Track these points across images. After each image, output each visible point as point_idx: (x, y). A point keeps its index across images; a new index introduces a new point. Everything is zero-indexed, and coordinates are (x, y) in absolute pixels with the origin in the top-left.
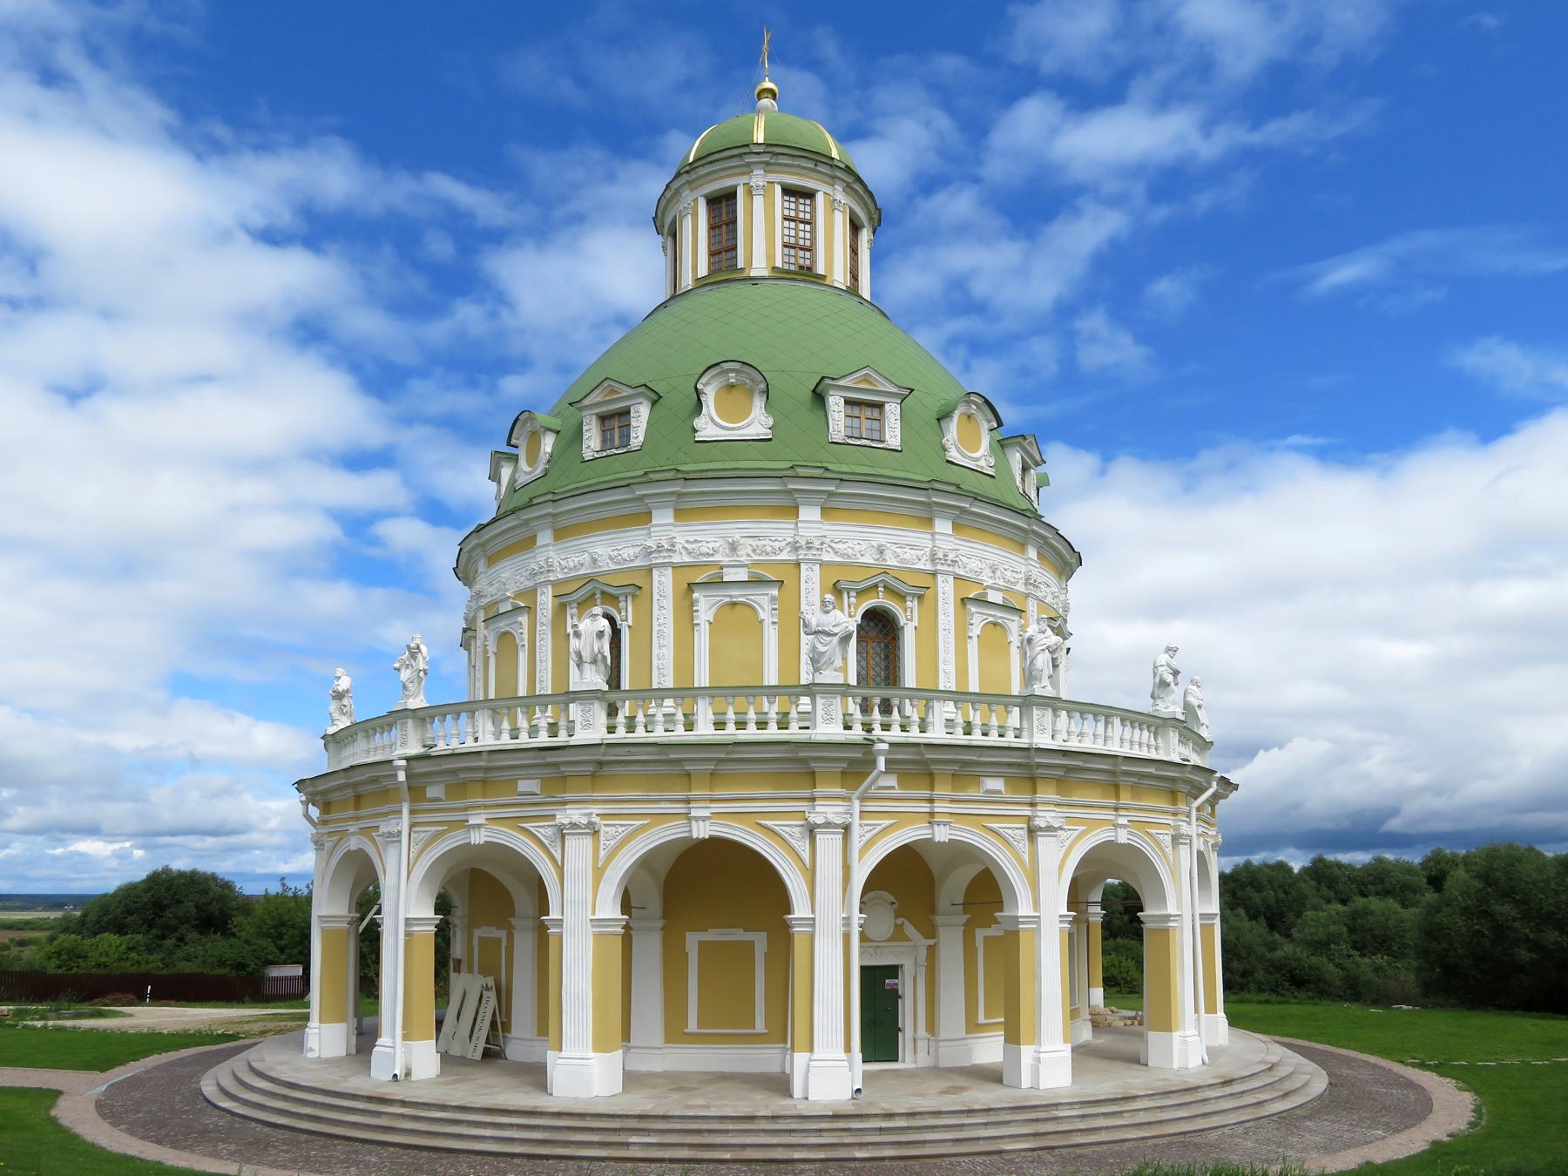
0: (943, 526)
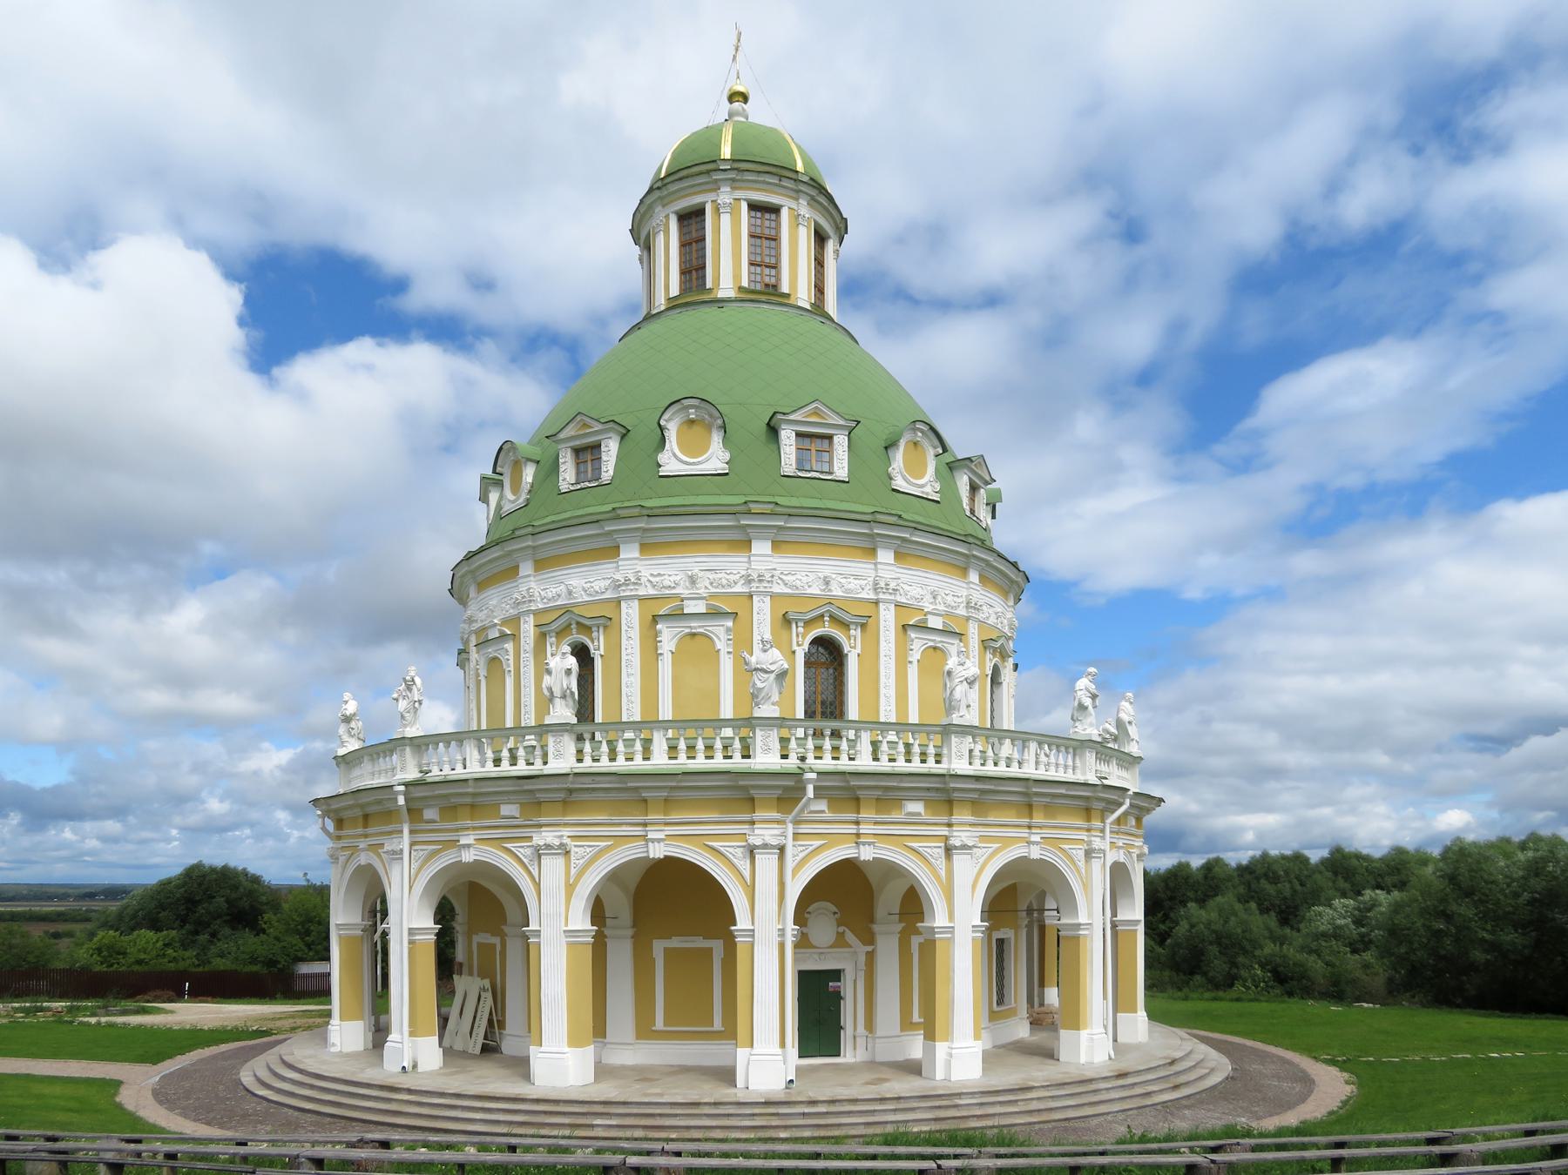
0: (885, 556)
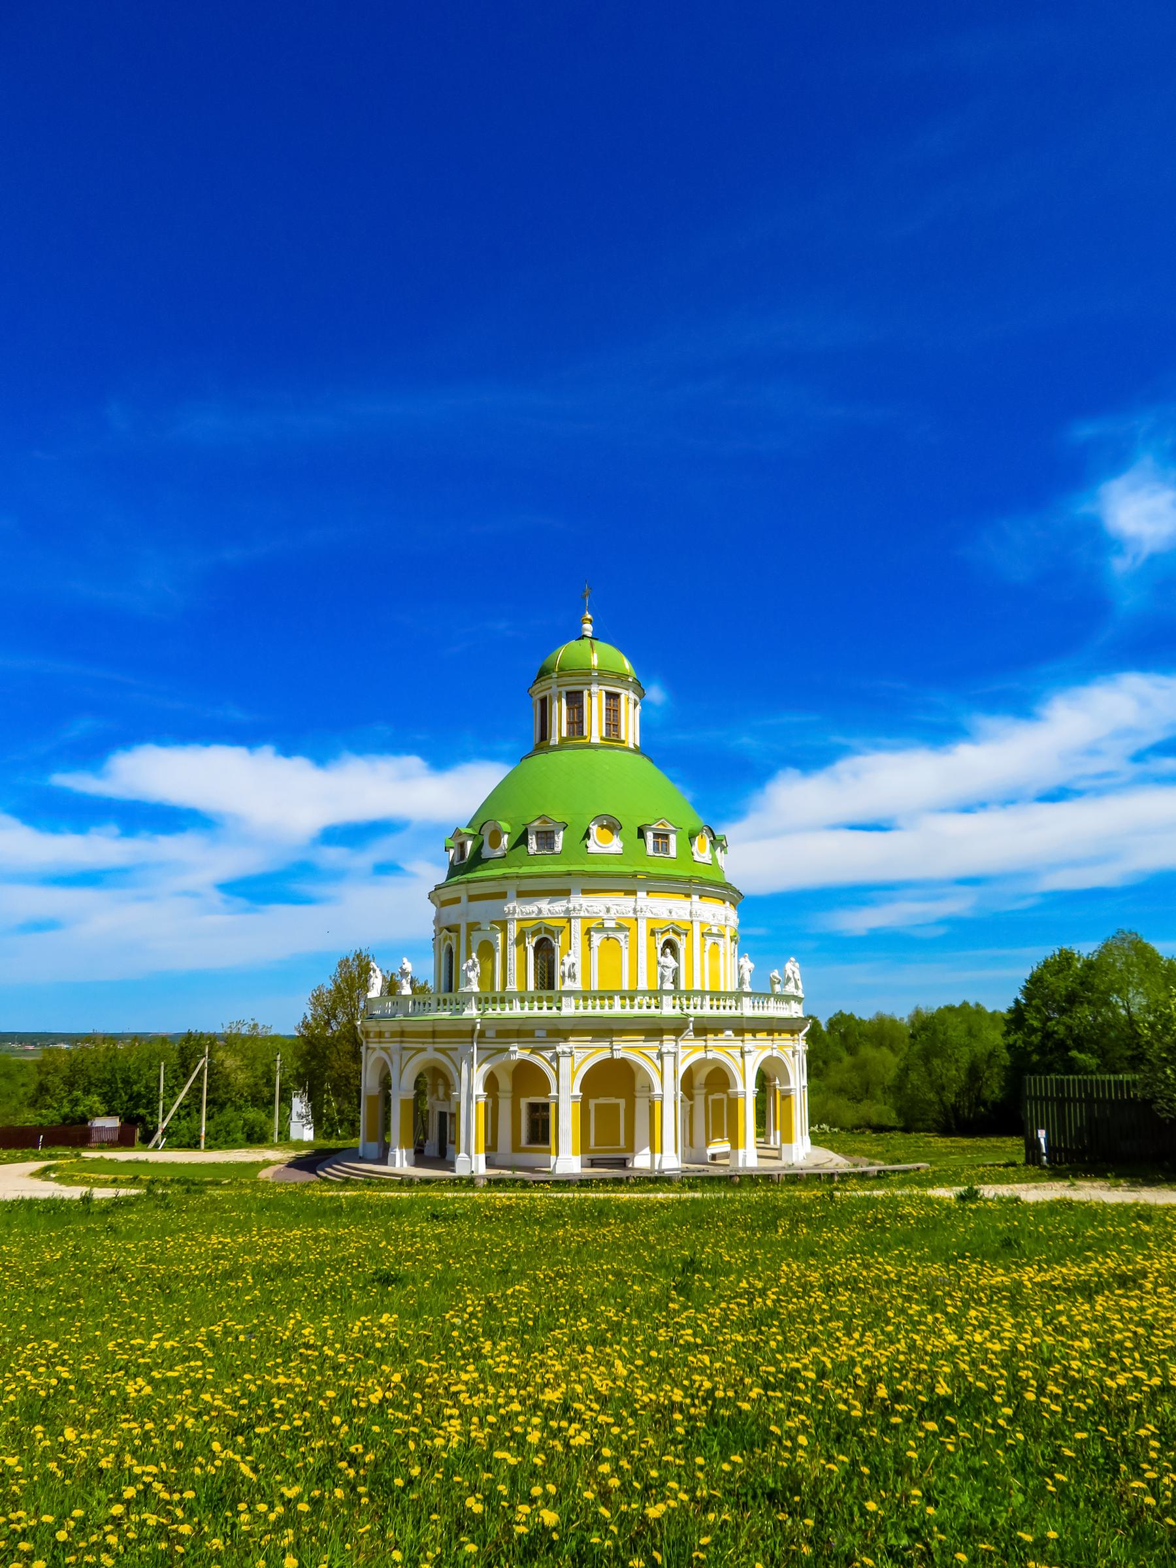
0: (695, 898)
